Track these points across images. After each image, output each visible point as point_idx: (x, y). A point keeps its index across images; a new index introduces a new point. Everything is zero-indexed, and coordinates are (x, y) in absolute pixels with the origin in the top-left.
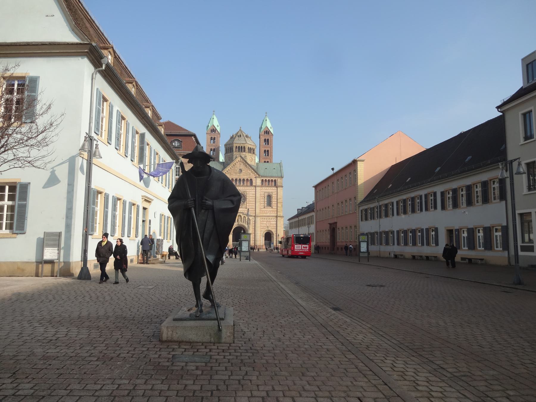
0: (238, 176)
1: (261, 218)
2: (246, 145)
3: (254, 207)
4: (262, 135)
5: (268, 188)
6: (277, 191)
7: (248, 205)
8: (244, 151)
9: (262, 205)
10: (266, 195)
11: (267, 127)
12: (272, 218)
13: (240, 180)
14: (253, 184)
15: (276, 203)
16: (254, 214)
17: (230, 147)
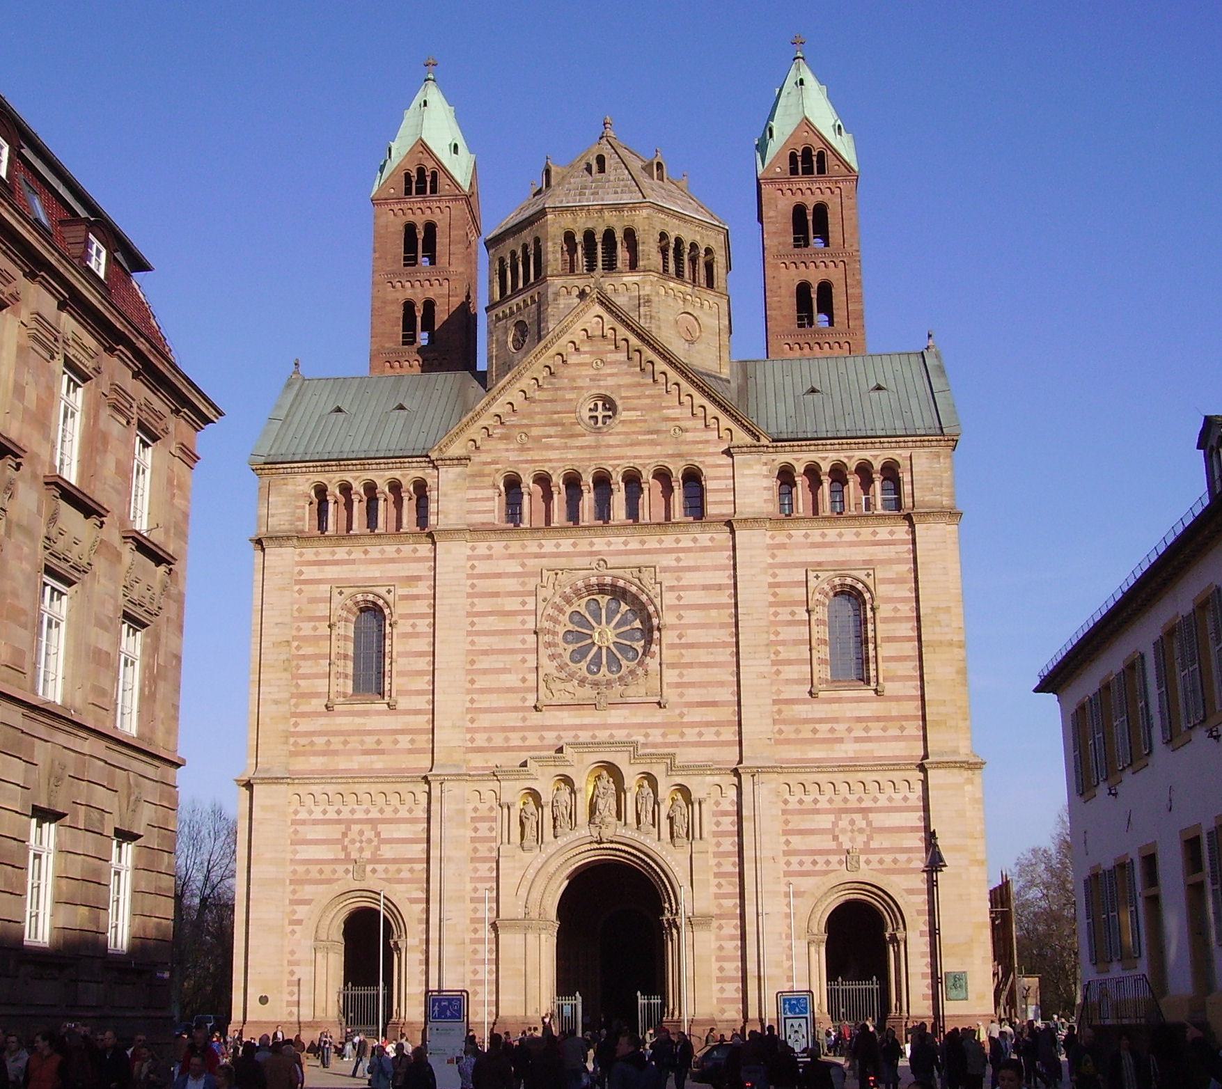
0: (585, 454)
1: (793, 779)
2: (641, 221)
3: (728, 695)
4: (772, 181)
5: (832, 533)
6: (914, 551)
7: (670, 676)
8: (633, 266)
9: (790, 672)
10: (822, 583)
11: (807, 119)
12: (883, 777)
13: (602, 482)
14: (711, 510)
15: (910, 648)
16: (732, 754)
17: (525, 247)
